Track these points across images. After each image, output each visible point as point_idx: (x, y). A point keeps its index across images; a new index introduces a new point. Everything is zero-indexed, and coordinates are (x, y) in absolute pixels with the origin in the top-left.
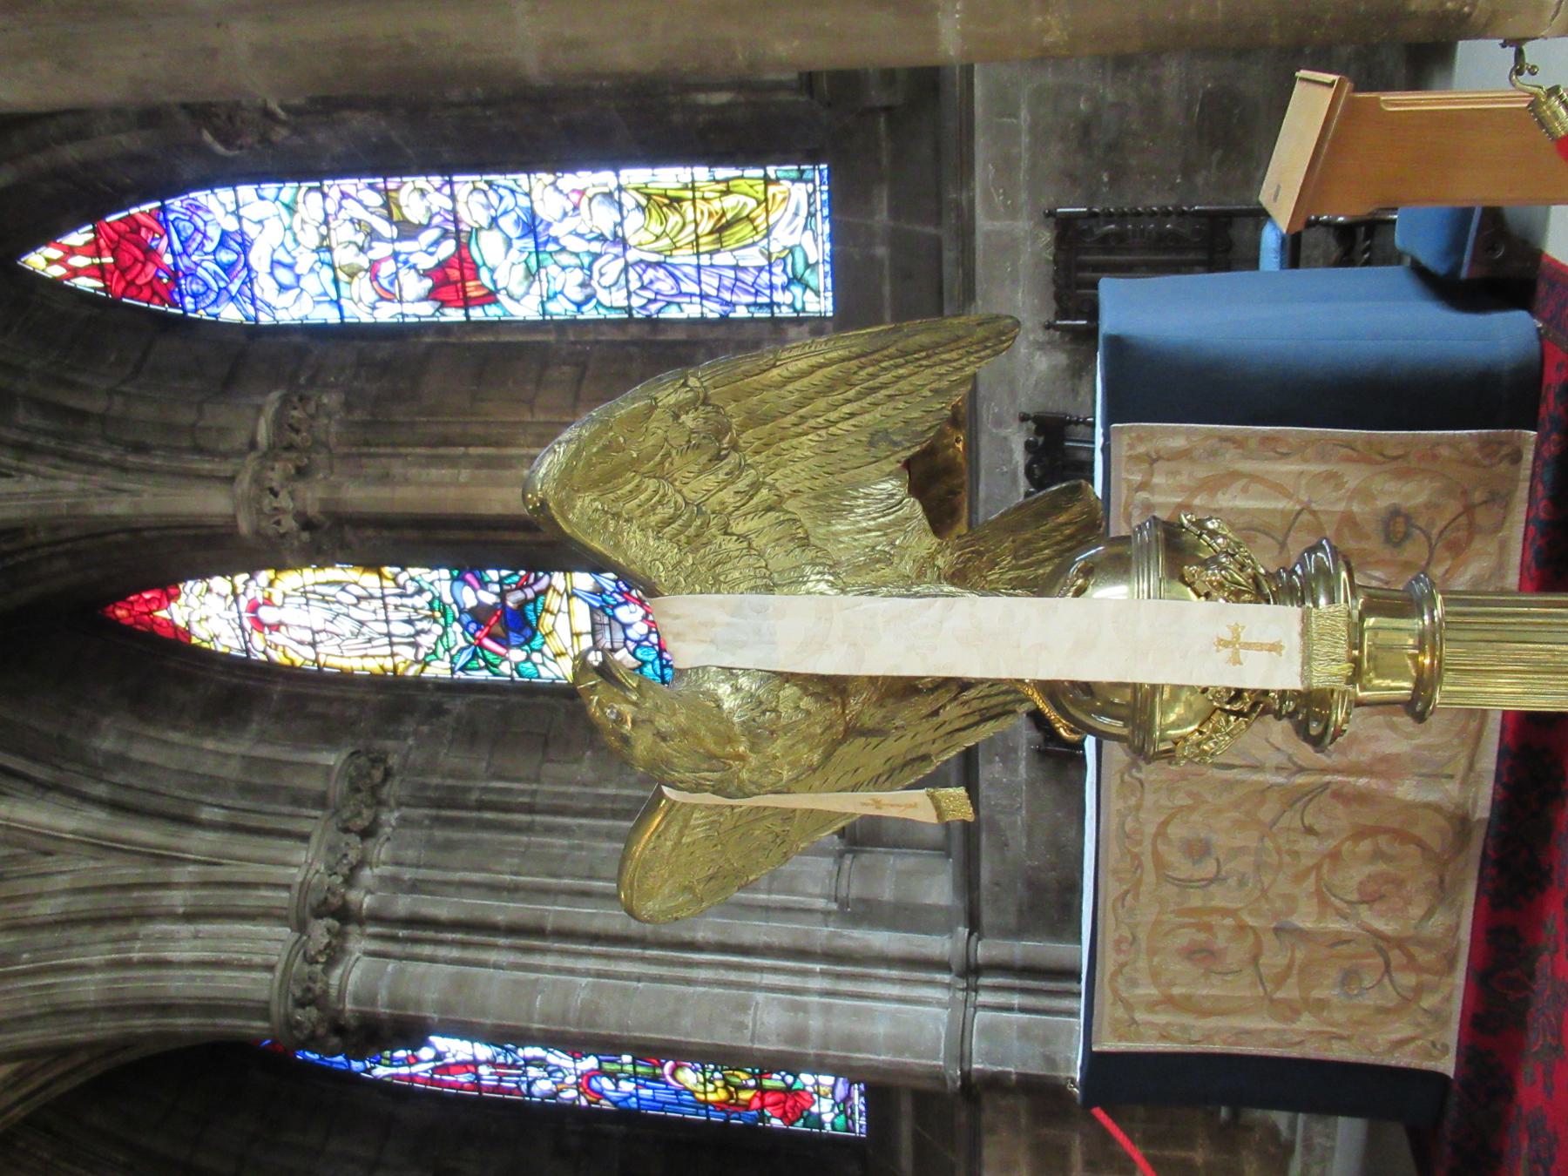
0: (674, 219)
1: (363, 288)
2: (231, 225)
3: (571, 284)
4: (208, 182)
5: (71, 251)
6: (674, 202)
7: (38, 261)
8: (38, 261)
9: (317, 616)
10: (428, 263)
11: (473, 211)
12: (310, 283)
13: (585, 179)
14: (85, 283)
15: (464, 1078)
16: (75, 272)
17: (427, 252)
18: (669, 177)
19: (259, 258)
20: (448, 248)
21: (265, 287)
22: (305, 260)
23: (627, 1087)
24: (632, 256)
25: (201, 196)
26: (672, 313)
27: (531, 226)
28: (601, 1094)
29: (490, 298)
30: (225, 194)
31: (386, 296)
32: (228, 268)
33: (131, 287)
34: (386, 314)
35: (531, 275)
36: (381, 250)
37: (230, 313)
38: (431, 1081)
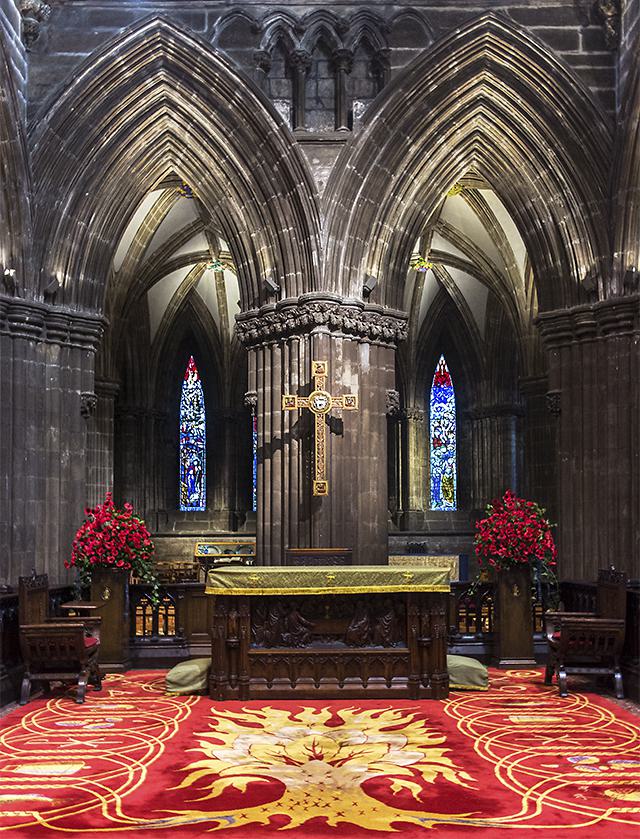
1: (437, 424)
6: (451, 484)
7: (442, 358)
8: (442, 358)
11: (450, 447)
12: (437, 414)
18: (455, 483)
19: (442, 405)
22: (442, 414)
27: (447, 458)
30: (453, 401)
31: (435, 429)
34: (432, 428)
35: (438, 456)
37: (432, 397)
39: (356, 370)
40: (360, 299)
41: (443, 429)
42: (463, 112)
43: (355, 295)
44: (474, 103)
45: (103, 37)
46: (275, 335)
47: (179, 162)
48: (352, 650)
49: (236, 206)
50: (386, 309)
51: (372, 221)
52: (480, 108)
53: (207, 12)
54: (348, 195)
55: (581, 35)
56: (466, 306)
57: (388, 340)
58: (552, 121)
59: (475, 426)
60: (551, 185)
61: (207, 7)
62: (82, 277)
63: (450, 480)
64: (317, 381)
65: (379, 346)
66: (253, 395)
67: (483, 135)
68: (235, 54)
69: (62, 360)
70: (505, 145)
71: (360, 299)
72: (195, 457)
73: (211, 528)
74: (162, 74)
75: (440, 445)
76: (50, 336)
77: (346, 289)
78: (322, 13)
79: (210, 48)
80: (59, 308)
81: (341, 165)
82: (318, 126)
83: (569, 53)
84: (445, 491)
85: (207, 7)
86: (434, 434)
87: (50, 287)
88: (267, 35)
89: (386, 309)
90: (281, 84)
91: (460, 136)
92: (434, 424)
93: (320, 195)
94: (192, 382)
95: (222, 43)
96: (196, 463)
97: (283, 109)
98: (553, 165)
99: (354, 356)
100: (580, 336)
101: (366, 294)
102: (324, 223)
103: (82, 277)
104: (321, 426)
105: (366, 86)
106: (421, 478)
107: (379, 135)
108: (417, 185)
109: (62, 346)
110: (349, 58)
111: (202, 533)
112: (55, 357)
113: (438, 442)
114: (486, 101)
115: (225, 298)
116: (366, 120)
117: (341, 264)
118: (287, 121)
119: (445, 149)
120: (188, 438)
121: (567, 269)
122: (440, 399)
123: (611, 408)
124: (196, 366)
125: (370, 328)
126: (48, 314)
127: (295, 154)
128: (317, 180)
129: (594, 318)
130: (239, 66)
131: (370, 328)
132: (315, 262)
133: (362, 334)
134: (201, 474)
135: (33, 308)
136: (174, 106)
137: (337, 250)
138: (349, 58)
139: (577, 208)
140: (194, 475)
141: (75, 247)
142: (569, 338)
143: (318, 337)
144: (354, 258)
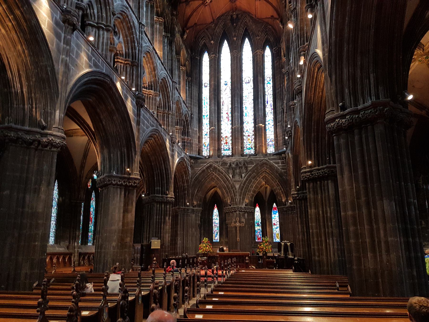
3: (275, 230)
7: (275, 204)
8: (275, 204)
9: (258, 215)
17: (276, 223)
18: (279, 235)
19: (275, 215)
27: (277, 228)
34: (273, 221)
37: (273, 213)
40: (245, 206)
41: (275, 221)
43: (244, 206)
44: (263, 172)
45: (202, 165)
50: (250, 207)
51: (246, 193)
54: (242, 190)
57: (250, 212)
63: (278, 234)
70: (269, 178)
71: (245, 206)
72: (216, 228)
74: (211, 170)
75: (275, 225)
77: (242, 205)
78: (237, 160)
80: (195, 208)
81: (240, 185)
82: (237, 178)
84: (277, 237)
86: (273, 222)
87: (194, 205)
89: (250, 207)
90: (231, 171)
91: (261, 177)
92: (273, 220)
93: (237, 190)
94: (216, 211)
95: (221, 166)
97: (231, 176)
98: (278, 182)
99: (244, 215)
101: (246, 205)
102: (238, 194)
104: (238, 229)
105: (245, 171)
107: (247, 180)
110: (242, 167)
114: (266, 171)
116: (244, 177)
118: (232, 178)
119: (259, 180)
120: (215, 224)
121: (282, 200)
124: (217, 206)
126: (193, 210)
130: (224, 169)
133: (245, 212)
135: (191, 209)
136: (213, 174)
137: (240, 199)
138: (242, 167)
139: (282, 189)
144: (243, 199)
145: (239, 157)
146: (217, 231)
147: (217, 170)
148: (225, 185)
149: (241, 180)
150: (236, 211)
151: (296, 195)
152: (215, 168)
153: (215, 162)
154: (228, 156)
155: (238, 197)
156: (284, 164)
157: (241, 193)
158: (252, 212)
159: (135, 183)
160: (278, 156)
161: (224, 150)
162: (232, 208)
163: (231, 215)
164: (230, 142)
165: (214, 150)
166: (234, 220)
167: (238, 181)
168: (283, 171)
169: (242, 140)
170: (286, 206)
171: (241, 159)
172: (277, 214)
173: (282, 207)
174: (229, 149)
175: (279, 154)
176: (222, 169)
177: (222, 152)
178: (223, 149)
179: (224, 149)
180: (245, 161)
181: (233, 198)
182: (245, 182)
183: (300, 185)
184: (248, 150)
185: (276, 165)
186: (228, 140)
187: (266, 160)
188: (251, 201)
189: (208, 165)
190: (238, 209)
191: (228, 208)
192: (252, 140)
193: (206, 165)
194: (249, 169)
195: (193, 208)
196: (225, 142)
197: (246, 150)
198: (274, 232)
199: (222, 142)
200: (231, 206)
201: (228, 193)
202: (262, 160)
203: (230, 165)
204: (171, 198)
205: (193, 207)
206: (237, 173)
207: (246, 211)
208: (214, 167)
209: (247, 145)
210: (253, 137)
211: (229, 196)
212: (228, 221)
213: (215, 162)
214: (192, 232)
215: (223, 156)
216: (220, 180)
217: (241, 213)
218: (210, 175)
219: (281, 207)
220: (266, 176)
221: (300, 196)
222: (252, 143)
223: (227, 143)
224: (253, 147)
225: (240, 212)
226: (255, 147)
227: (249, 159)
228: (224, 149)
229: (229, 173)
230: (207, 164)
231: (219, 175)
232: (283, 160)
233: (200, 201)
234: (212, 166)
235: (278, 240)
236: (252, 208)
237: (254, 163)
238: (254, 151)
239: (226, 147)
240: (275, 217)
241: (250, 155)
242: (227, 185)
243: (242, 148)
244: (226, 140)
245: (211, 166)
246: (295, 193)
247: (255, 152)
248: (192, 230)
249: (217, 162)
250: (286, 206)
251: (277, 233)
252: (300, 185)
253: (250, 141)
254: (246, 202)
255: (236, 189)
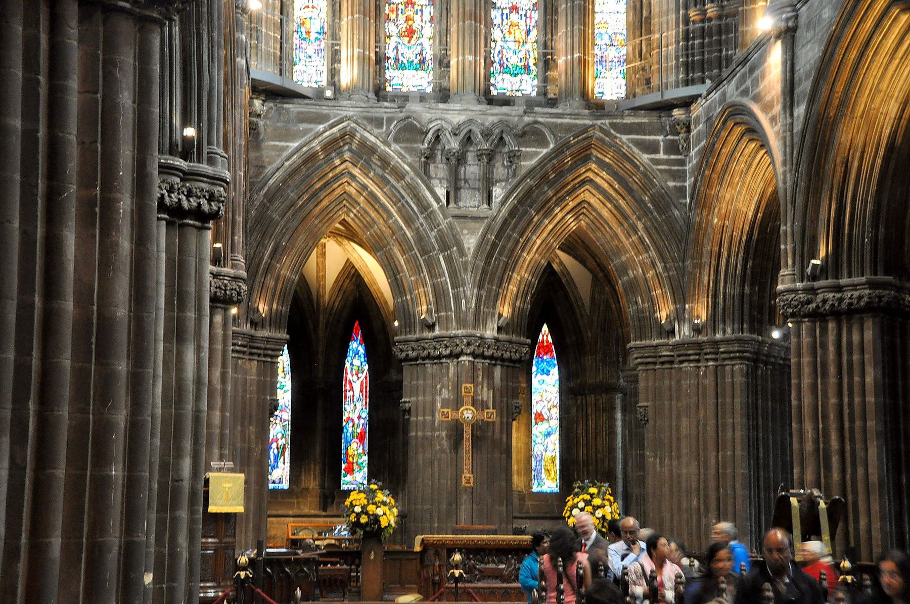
0: (550, 462)
2: (551, 373)
4: (559, 369)
5: (547, 336)
7: (545, 328)
8: (545, 328)
10: (543, 413)
13: (557, 445)
14: (540, 337)
15: (348, 387)
16: (543, 336)
18: (557, 462)
20: (546, 417)
21: (539, 377)
23: (350, 430)
24: (544, 453)
25: (557, 367)
26: (533, 459)
28: (347, 422)
29: (536, 423)
31: (537, 403)
32: (543, 370)
33: (539, 348)
34: (534, 402)
36: (546, 403)
37: (534, 368)
38: (346, 379)
39: (491, 386)
40: (496, 335)
42: (574, 189)
43: (490, 332)
45: (305, 132)
46: (429, 357)
47: (352, 215)
48: (505, 585)
49: (399, 255)
52: (588, 187)
53: (385, 116)
55: (662, 144)
56: (571, 281)
57: (514, 362)
58: (640, 203)
59: (579, 401)
60: (640, 247)
61: (386, 113)
62: (275, 306)
64: (465, 399)
65: (508, 366)
66: (407, 400)
67: (589, 203)
68: (409, 150)
69: (259, 373)
70: (605, 213)
71: (496, 335)
73: (299, 508)
74: (347, 155)
75: (543, 420)
76: (251, 354)
78: (470, 121)
79: (389, 146)
82: (470, 202)
83: (653, 156)
85: (386, 113)
86: (536, 408)
87: (256, 318)
88: (430, 135)
89: (514, 338)
90: (439, 169)
91: (572, 205)
92: (535, 397)
95: (397, 140)
96: (279, 436)
97: (441, 192)
98: (642, 233)
99: (489, 375)
100: (663, 363)
101: (500, 329)
103: (275, 306)
104: (467, 433)
106: (522, 456)
107: (512, 213)
108: (539, 242)
109: (258, 361)
111: (291, 513)
112: (254, 370)
113: (540, 417)
114: (591, 181)
115: (324, 267)
116: (503, 203)
117: (482, 307)
118: (444, 201)
119: (560, 216)
122: (543, 370)
123: (685, 422)
125: (502, 355)
126: (252, 338)
127: (451, 227)
128: (466, 246)
129: (672, 350)
130: (409, 159)
131: (502, 355)
132: (464, 308)
133: (496, 359)
134: (284, 448)
136: (353, 177)
137: (479, 298)
139: (660, 266)
140: (277, 448)
141: (272, 283)
142: (655, 363)
143: (464, 364)
145: (479, 107)
146: (281, 442)
147: (375, 159)
148: (409, 234)
149: (490, 212)
150: (457, 356)
151: (802, 296)
152: (365, 153)
153: (370, 120)
154: (422, 98)
155: (470, 290)
156: (678, 152)
157: (484, 272)
158: (519, 361)
159: (211, 198)
160: (655, 113)
161: (399, 65)
162: (434, 338)
163: (429, 370)
164: (428, 31)
165: (363, 59)
166: (445, 394)
167: (475, 219)
168: (671, 184)
169: (489, 24)
170: (672, 341)
171: (493, 116)
172: (555, 372)
173: (656, 342)
174: (422, 62)
175: (665, 107)
176: (400, 155)
177: (389, 74)
178: (391, 61)
179: (397, 60)
180: (505, 126)
181: (445, 293)
182: (505, 223)
183: (822, 253)
184: (507, 76)
185: (645, 157)
186: (417, 18)
187: (602, 130)
188: (521, 311)
189: (335, 130)
190: (469, 344)
191: (418, 340)
192: (528, 32)
193: (325, 132)
194: (527, 164)
195: (253, 332)
196: (404, 26)
197: (499, 77)
198: (537, 449)
199: (391, 28)
200: (431, 327)
201: (420, 271)
202: (586, 129)
203: (437, 138)
204: (235, 278)
205: (254, 324)
206: (466, 181)
207: (499, 354)
208: (363, 144)
209: (508, 54)
210: (535, 16)
211: (424, 285)
212: (413, 399)
213: (370, 120)
214: (243, 440)
215: (405, 98)
216: (382, 206)
217: (480, 363)
218: (336, 178)
219: (647, 342)
220: (593, 201)
221: (825, 301)
222: (529, 46)
223: (410, 32)
224: (531, 62)
225: (474, 355)
226: (547, 62)
227: (527, 119)
228: (397, 60)
229: (429, 177)
230: (332, 126)
231: (383, 182)
232: (678, 134)
233: (282, 300)
234: (352, 136)
235: (549, 483)
236: (521, 344)
237: (550, 137)
238: (536, 82)
239: (409, 53)
240: (544, 386)
241: (530, 104)
242: (417, 232)
243: (489, 63)
244: (408, 19)
245: (346, 136)
246: (799, 285)
247: (543, 93)
248: (243, 432)
249: (378, 122)
250: (672, 341)
251: (549, 454)
252: (822, 253)
253: (520, 34)
254: (500, 316)
255: (462, 252)
